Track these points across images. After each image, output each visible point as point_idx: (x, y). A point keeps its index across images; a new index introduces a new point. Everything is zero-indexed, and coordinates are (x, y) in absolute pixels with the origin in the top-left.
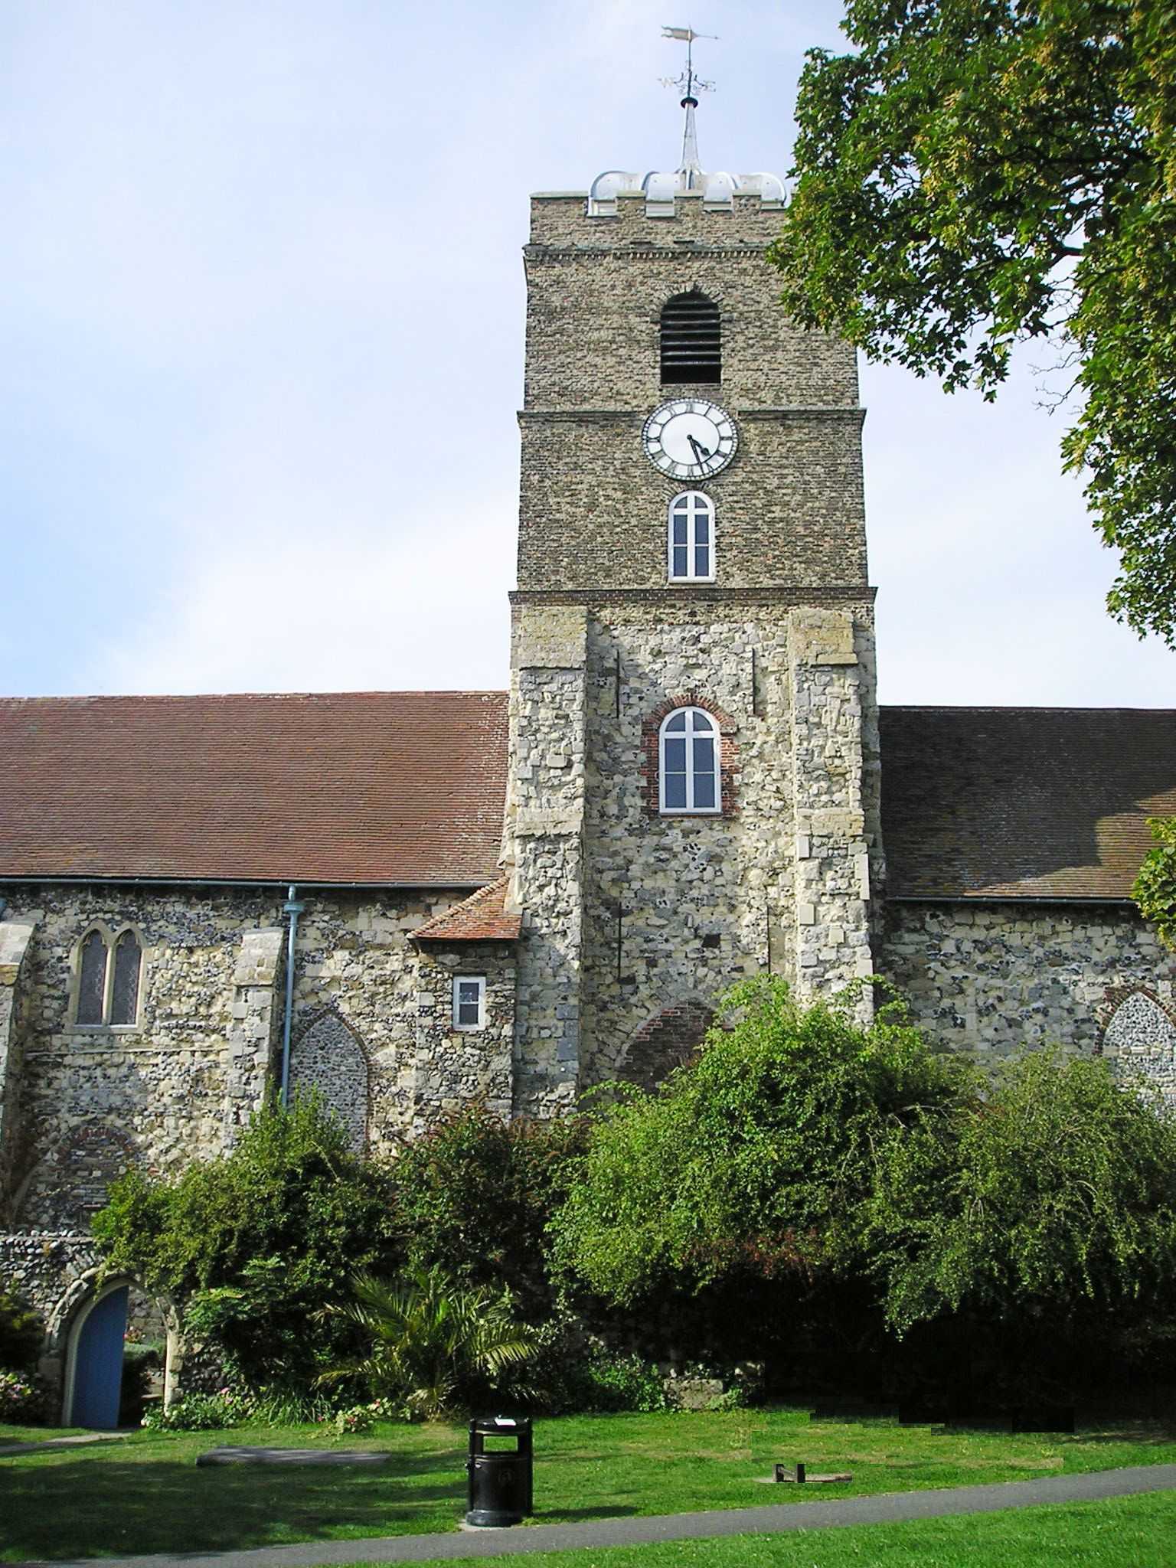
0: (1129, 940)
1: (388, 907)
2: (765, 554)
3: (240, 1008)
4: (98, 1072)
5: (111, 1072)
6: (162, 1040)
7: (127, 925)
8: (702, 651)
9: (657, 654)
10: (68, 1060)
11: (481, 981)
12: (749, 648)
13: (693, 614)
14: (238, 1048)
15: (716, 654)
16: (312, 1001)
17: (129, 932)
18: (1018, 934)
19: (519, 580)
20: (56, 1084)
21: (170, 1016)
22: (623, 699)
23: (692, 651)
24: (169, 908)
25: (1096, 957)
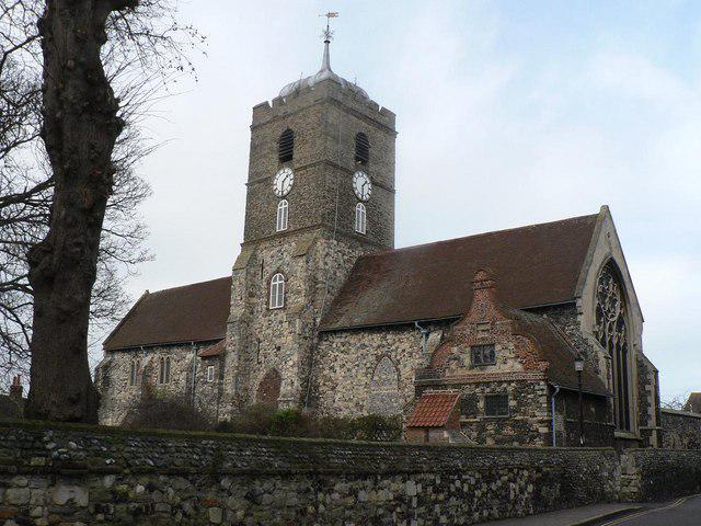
0: (384, 338)
18: (353, 339)
25: (374, 345)
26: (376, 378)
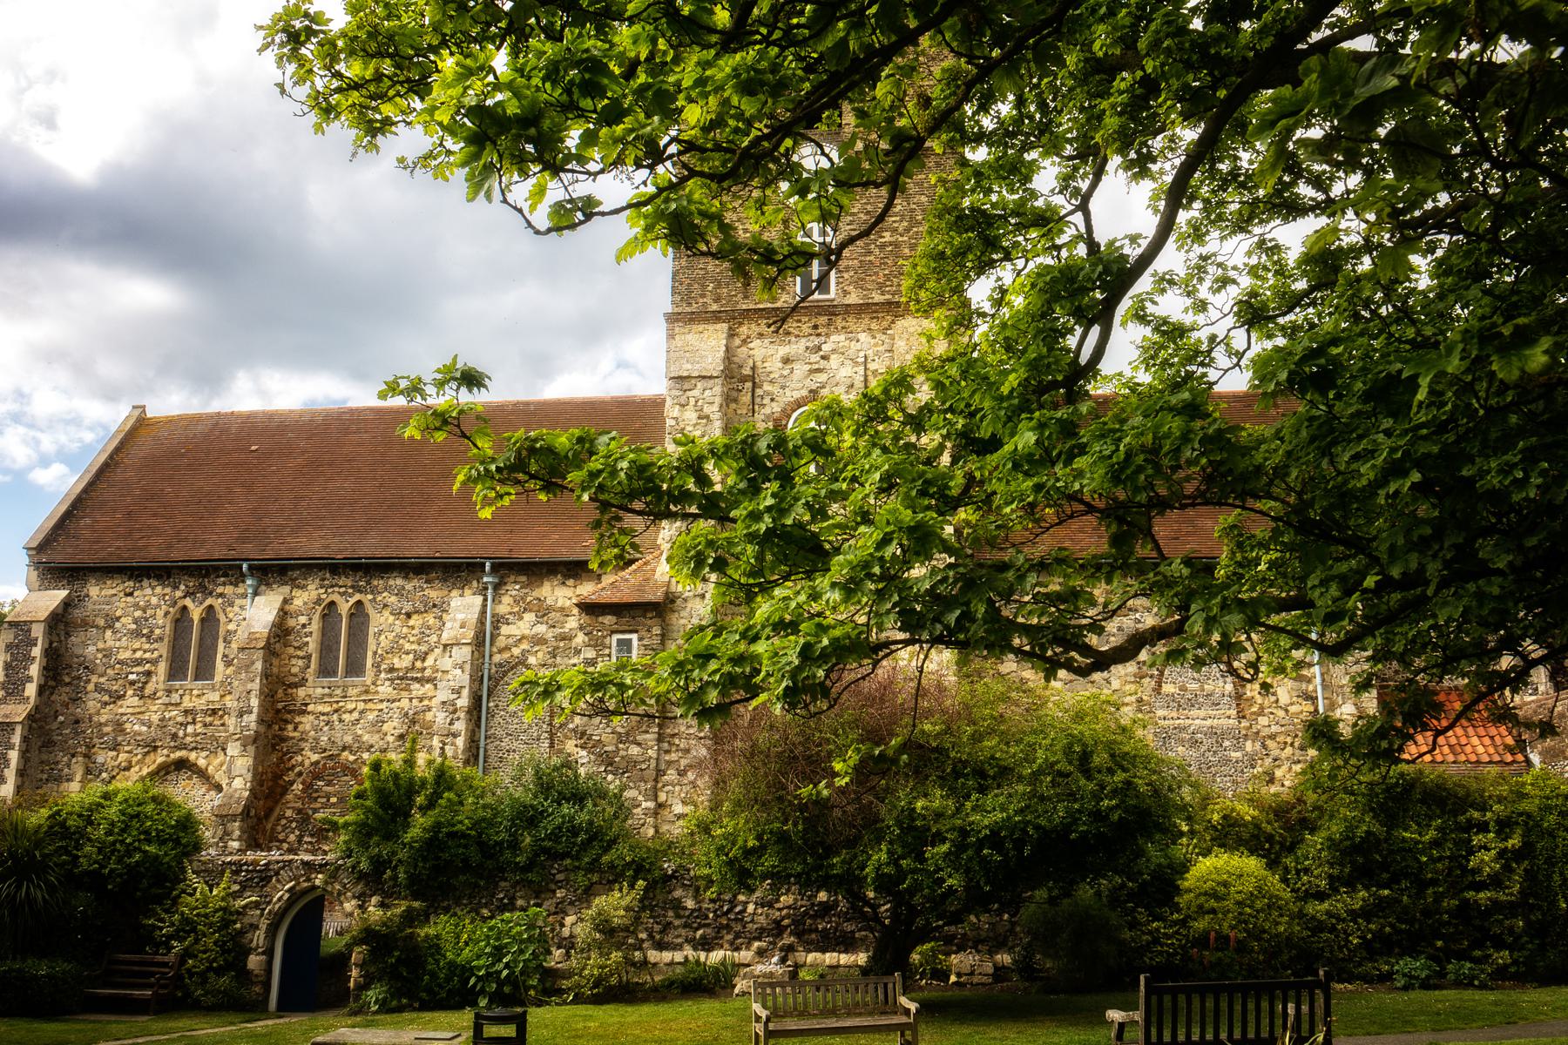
1: (567, 576)
2: (876, 274)
3: (446, 663)
4: (335, 717)
5: (345, 716)
6: (385, 690)
7: (357, 597)
8: (823, 358)
9: (786, 361)
10: (310, 708)
11: (634, 637)
12: (862, 354)
13: (816, 327)
14: (443, 695)
15: (835, 361)
16: (506, 655)
17: (359, 603)
19: (673, 303)
20: (300, 728)
21: (392, 670)
22: (758, 400)
23: (815, 358)
24: (391, 582)
26: (1168, 688)
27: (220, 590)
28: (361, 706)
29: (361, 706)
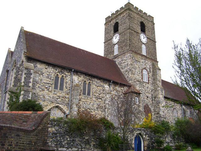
4: (86, 102)
5: (87, 103)
6: (94, 99)
7: (89, 81)
10: (81, 100)
17: (90, 82)
21: (95, 96)
27: (65, 73)
28: (90, 101)
29: (90, 101)
